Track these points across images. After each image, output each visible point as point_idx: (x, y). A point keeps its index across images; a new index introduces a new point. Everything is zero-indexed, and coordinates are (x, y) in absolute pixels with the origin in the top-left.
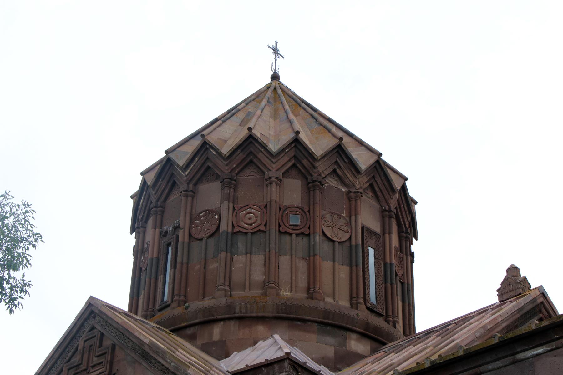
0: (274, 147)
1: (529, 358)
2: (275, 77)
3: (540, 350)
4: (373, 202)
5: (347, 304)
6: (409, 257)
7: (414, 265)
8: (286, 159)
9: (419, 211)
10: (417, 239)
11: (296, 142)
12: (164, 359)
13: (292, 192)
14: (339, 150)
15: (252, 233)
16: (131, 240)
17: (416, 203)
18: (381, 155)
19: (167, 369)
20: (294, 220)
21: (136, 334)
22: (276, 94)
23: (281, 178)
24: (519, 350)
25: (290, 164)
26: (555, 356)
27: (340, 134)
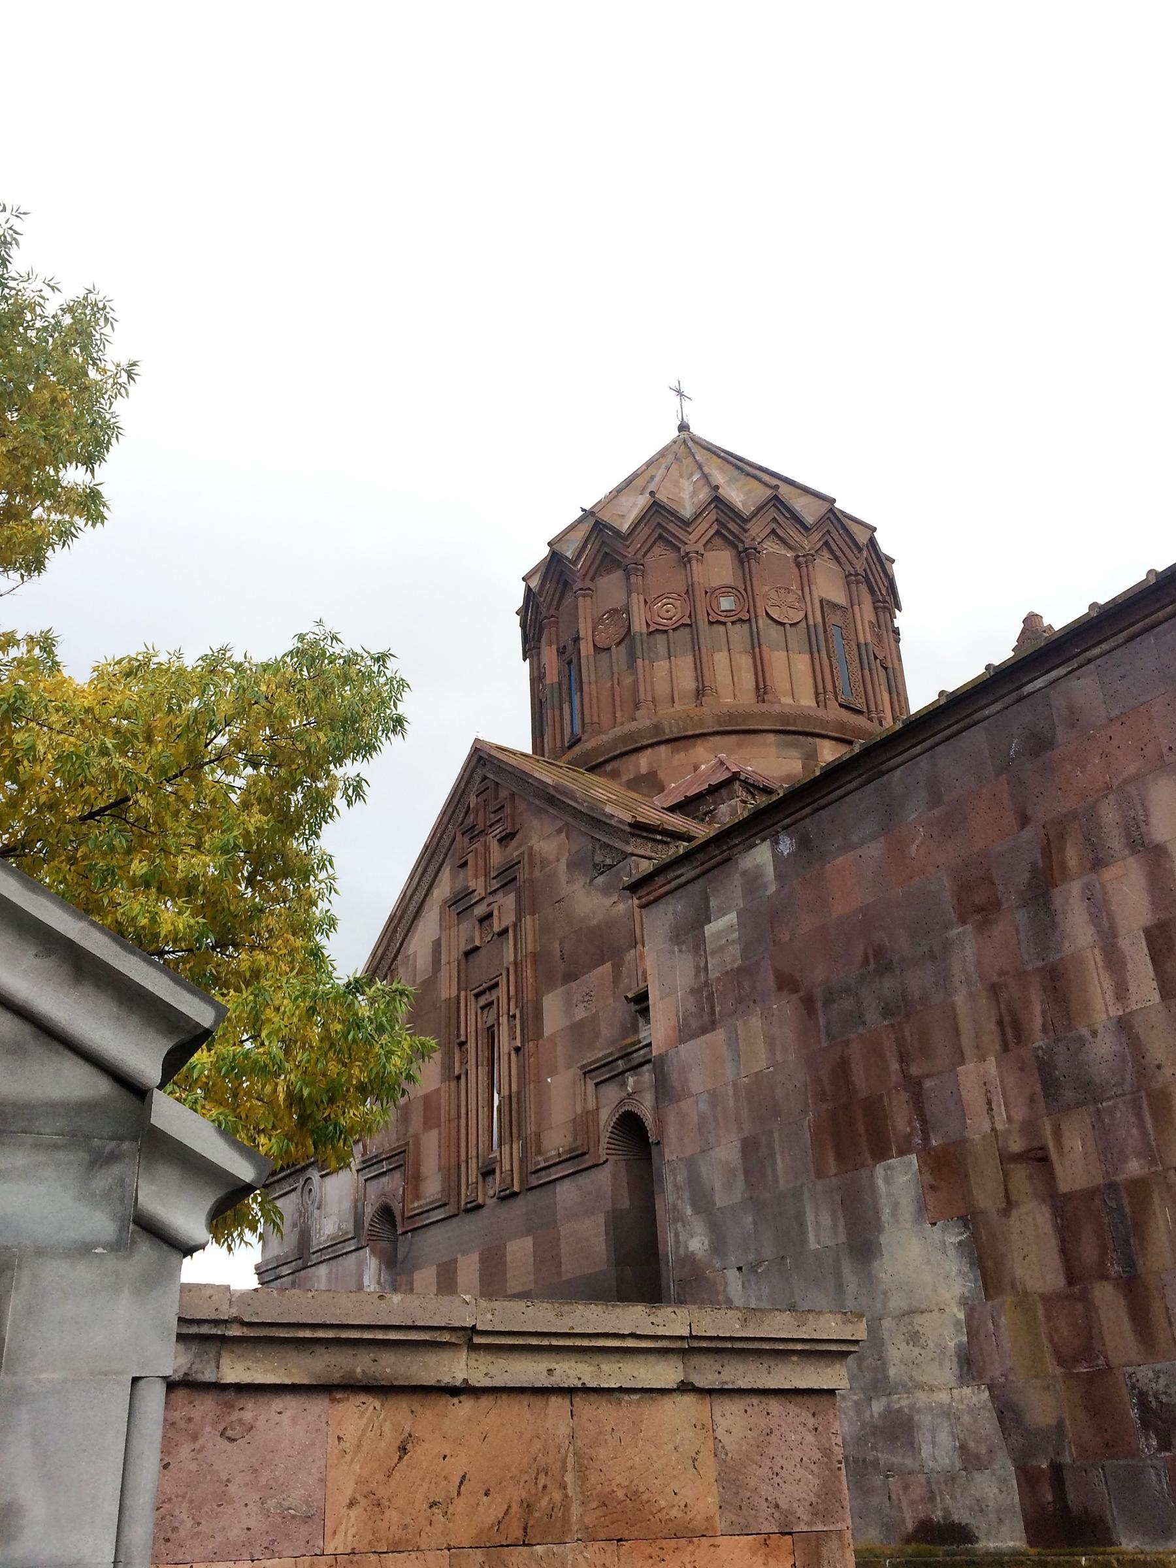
0: (687, 512)
2: (683, 427)
3: (1054, 674)
4: (833, 565)
6: (891, 634)
7: (901, 644)
8: (705, 525)
9: (897, 570)
11: (717, 501)
12: (576, 801)
13: (719, 567)
14: (776, 501)
15: (674, 630)
18: (834, 500)
20: (726, 603)
21: (536, 775)
24: (1026, 680)
25: (712, 532)
27: (775, 482)
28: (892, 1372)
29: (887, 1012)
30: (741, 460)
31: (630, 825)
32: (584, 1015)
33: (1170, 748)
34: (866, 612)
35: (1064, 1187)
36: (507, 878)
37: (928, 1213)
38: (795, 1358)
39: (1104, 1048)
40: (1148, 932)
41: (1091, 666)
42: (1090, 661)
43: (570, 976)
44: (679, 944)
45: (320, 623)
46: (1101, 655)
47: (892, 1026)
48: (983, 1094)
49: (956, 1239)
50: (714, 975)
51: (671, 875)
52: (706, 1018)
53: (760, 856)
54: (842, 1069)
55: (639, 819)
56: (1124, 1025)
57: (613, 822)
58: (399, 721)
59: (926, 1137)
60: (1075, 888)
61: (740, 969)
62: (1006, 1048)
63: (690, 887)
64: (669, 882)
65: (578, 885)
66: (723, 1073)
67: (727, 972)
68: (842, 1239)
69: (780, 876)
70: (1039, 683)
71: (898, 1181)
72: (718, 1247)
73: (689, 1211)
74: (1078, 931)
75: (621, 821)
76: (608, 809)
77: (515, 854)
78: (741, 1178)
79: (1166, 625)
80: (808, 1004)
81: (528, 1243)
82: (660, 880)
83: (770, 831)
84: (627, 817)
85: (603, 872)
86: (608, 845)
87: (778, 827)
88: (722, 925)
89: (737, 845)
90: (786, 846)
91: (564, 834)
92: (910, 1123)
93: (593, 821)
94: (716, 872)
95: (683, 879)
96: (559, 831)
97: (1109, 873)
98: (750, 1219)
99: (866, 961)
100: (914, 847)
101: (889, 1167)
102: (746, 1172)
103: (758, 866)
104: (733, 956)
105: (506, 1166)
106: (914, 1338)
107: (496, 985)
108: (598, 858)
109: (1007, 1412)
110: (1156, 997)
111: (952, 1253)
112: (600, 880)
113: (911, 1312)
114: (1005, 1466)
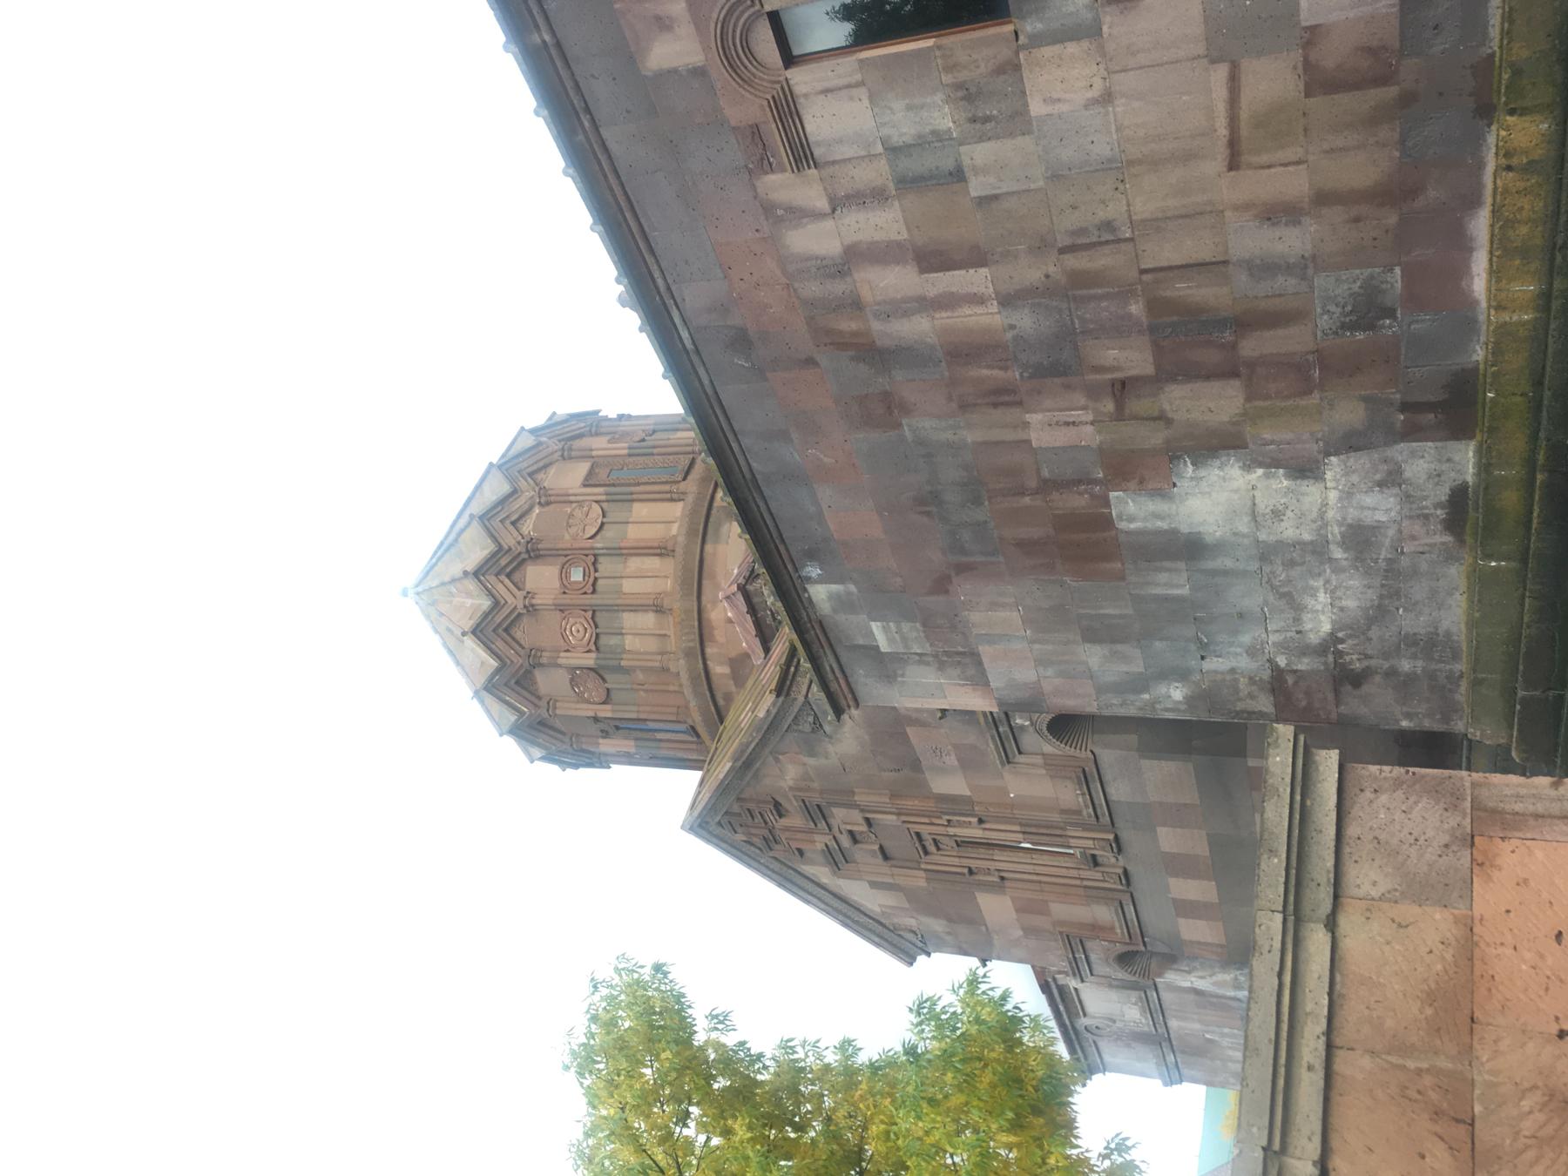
3: (677, 320)
4: (552, 471)
5: (681, 504)
7: (634, 413)
8: (500, 587)
11: (479, 573)
13: (542, 578)
20: (577, 575)
21: (721, 776)
25: (507, 581)
28: (1307, 537)
29: (977, 501)
30: (442, 543)
32: (953, 757)
35: (1150, 370)
36: (817, 813)
37: (1164, 491)
38: (1308, 803)
39: (1025, 320)
40: (923, 271)
42: (669, 289)
43: (916, 766)
44: (896, 676)
46: (665, 279)
47: (990, 498)
48: (1058, 428)
49: (1190, 468)
50: (928, 649)
51: (830, 676)
52: (967, 660)
53: (820, 593)
54: (1027, 547)
55: (773, 686)
56: (1007, 301)
57: (774, 711)
58: (658, 968)
59: (1096, 482)
60: (876, 326)
61: (924, 625)
62: (1020, 403)
63: (844, 660)
65: (831, 748)
66: (1018, 648)
67: (927, 637)
68: (1181, 565)
69: (840, 581)
70: (685, 335)
71: (1133, 511)
72: (1182, 675)
73: (1146, 696)
74: (918, 328)
75: (774, 704)
76: (761, 715)
78: (1119, 647)
80: (962, 569)
81: (1162, 832)
82: (834, 686)
83: (797, 582)
84: (769, 699)
87: (795, 576)
88: (880, 636)
90: (813, 571)
92: (1080, 494)
93: (771, 729)
94: (831, 635)
95: (835, 666)
96: (777, 760)
97: (866, 295)
98: (1157, 643)
99: (928, 514)
101: (1120, 517)
102: (1114, 641)
104: (912, 630)
105: (1090, 843)
106: (1277, 514)
107: (918, 834)
108: (807, 728)
109: (1350, 443)
110: (984, 271)
111: (1202, 473)
112: (827, 728)
113: (1254, 515)
114: (1400, 451)
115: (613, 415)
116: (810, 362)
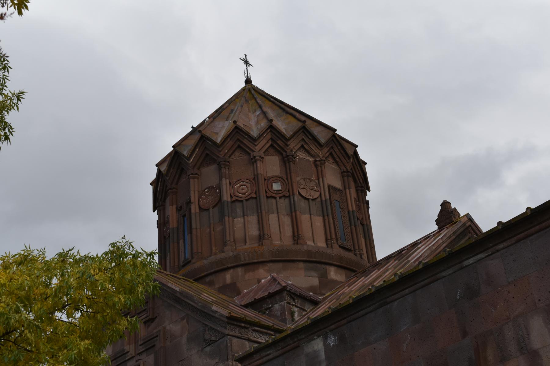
0: (255, 133)
1: (472, 264)
2: (248, 81)
4: (334, 166)
5: (324, 245)
6: (365, 205)
7: (370, 210)
8: (264, 141)
10: (369, 191)
11: (272, 128)
14: (304, 130)
15: (247, 200)
16: (155, 217)
17: (366, 164)
18: (336, 130)
19: (196, 308)
20: (276, 186)
21: (169, 285)
22: (250, 93)
23: (263, 156)
25: (268, 145)
26: (492, 260)
27: (303, 118)
31: (227, 317)
33: (539, 300)
34: (352, 193)
41: (498, 254)
42: (498, 251)
45: (124, 237)
51: (263, 354)
55: (233, 314)
57: (217, 316)
64: (262, 358)
69: (328, 357)
70: (471, 261)
75: (222, 315)
76: (214, 308)
77: (155, 331)
79: (535, 235)
82: (257, 356)
84: (225, 313)
85: (209, 345)
86: (213, 329)
89: (303, 339)
91: (185, 320)
93: (204, 313)
95: (271, 357)
96: (182, 319)
100: (405, 345)
103: (315, 351)
108: (207, 337)
112: (208, 349)
115: (368, 198)
116: (465, 334)
